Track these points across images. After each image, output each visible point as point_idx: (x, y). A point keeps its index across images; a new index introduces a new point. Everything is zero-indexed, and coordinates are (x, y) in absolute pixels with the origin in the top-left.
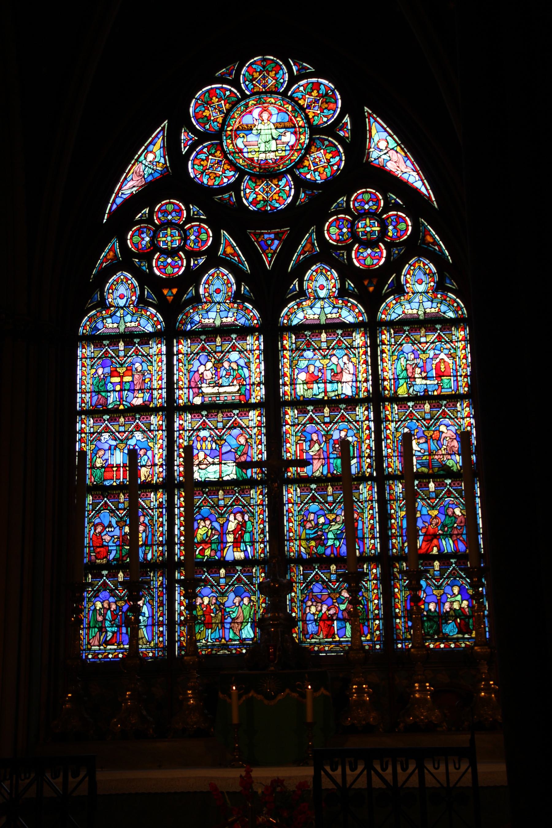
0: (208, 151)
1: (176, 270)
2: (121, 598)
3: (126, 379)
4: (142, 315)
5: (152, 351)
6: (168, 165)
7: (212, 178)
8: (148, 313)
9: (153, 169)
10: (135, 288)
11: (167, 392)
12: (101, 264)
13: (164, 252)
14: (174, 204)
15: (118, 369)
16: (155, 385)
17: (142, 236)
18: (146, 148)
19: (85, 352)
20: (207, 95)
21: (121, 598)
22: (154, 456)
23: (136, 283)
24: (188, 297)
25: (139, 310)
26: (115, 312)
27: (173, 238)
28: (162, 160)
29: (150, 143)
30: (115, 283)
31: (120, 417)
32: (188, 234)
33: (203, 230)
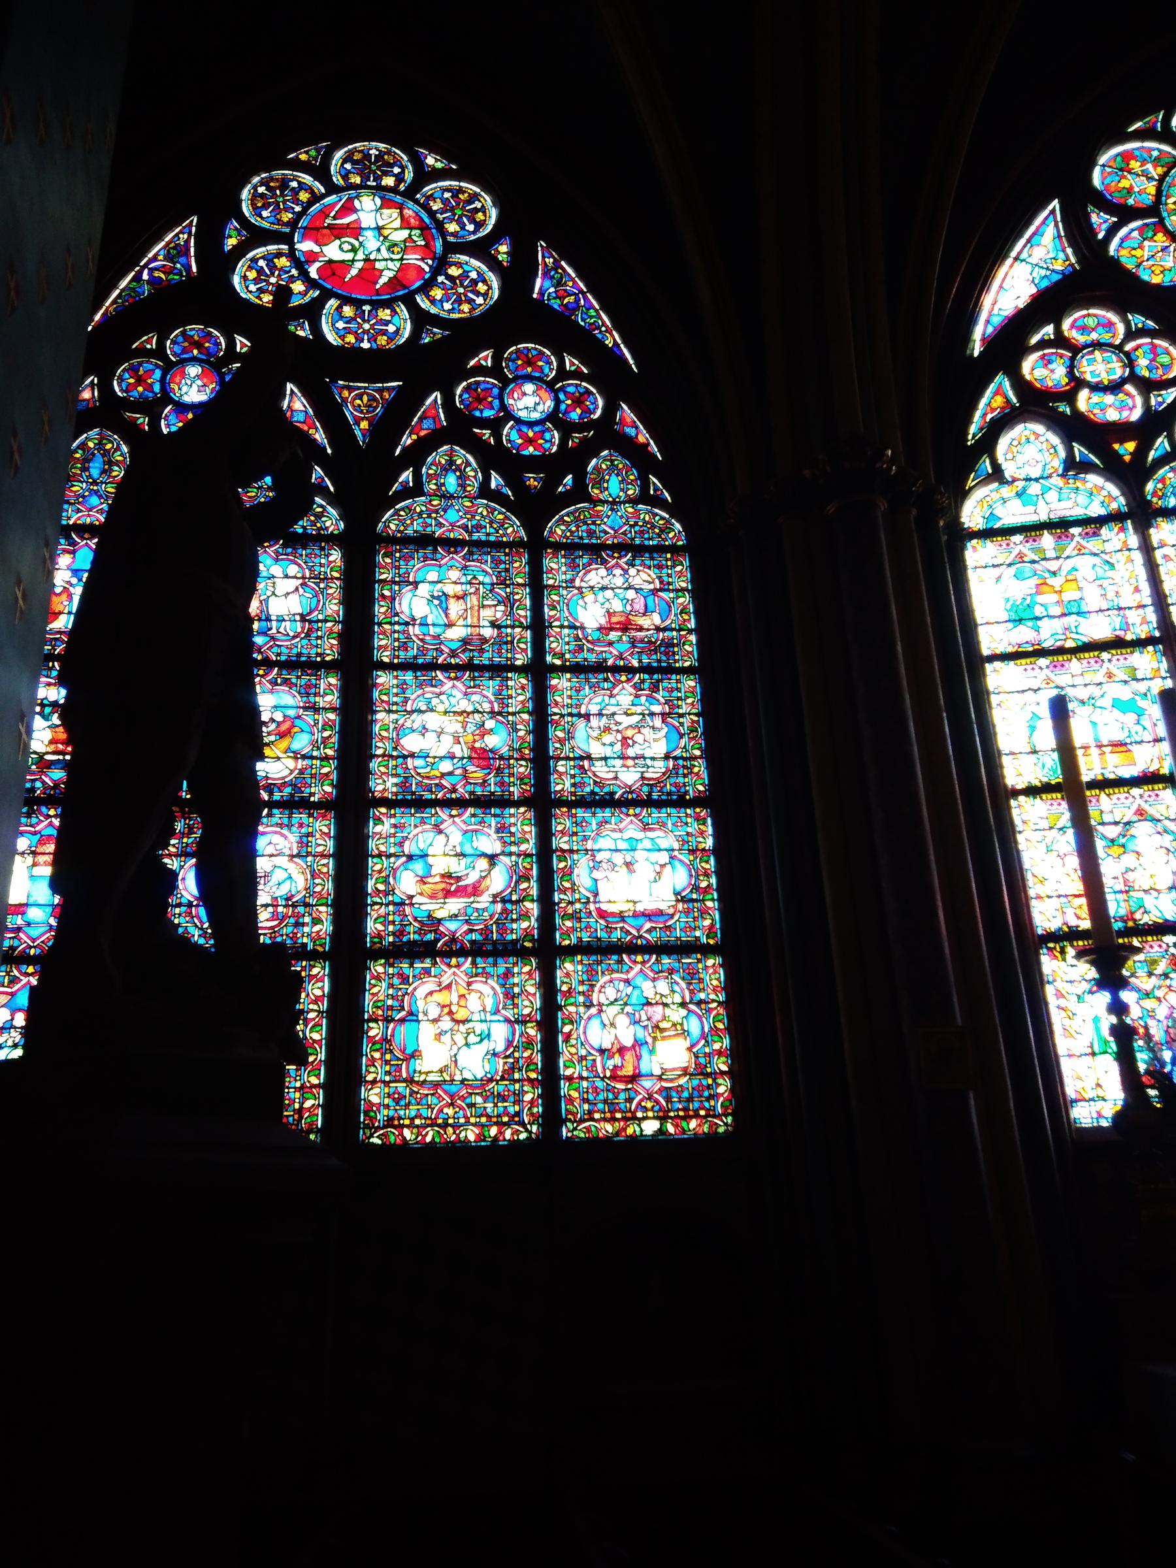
0: (1141, 234)
1: (1125, 414)
2: (1147, 995)
3: (1066, 597)
4: (1077, 489)
5: (1108, 547)
6: (1073, 260)
7: (1157, 272)
8: (1089, 485)
9: (1047, 269)
10: (1054, 447)
11: (1156, 611)
12: (985, 415)
13: (1096, 388)
14: (1095, 316)
15: (1048, 581)
16: (1128, 599)
17: (1050, 366)
18: (1029, 241)
19: (976, 555)
20: (1119, 159)
21: (1147, 995)
22: (1155, 725)
23: (1055, 440)
24: (1159, 453)
25: (1071, 481)
26: (1024, 490)
27: (1109, 366)
28: (1061, 256)
29: (1034, 234)
30: (1015, 443)
31: (1070, 660)
32: (1134, 358)
33: (1159, 350)
